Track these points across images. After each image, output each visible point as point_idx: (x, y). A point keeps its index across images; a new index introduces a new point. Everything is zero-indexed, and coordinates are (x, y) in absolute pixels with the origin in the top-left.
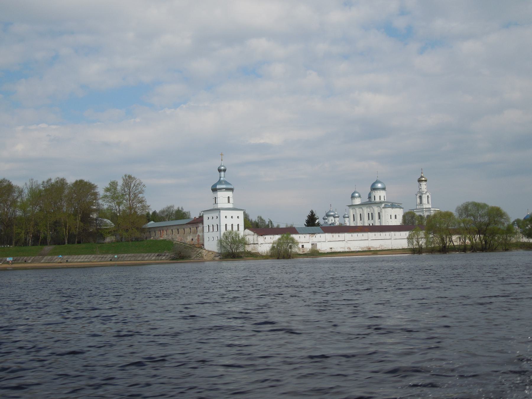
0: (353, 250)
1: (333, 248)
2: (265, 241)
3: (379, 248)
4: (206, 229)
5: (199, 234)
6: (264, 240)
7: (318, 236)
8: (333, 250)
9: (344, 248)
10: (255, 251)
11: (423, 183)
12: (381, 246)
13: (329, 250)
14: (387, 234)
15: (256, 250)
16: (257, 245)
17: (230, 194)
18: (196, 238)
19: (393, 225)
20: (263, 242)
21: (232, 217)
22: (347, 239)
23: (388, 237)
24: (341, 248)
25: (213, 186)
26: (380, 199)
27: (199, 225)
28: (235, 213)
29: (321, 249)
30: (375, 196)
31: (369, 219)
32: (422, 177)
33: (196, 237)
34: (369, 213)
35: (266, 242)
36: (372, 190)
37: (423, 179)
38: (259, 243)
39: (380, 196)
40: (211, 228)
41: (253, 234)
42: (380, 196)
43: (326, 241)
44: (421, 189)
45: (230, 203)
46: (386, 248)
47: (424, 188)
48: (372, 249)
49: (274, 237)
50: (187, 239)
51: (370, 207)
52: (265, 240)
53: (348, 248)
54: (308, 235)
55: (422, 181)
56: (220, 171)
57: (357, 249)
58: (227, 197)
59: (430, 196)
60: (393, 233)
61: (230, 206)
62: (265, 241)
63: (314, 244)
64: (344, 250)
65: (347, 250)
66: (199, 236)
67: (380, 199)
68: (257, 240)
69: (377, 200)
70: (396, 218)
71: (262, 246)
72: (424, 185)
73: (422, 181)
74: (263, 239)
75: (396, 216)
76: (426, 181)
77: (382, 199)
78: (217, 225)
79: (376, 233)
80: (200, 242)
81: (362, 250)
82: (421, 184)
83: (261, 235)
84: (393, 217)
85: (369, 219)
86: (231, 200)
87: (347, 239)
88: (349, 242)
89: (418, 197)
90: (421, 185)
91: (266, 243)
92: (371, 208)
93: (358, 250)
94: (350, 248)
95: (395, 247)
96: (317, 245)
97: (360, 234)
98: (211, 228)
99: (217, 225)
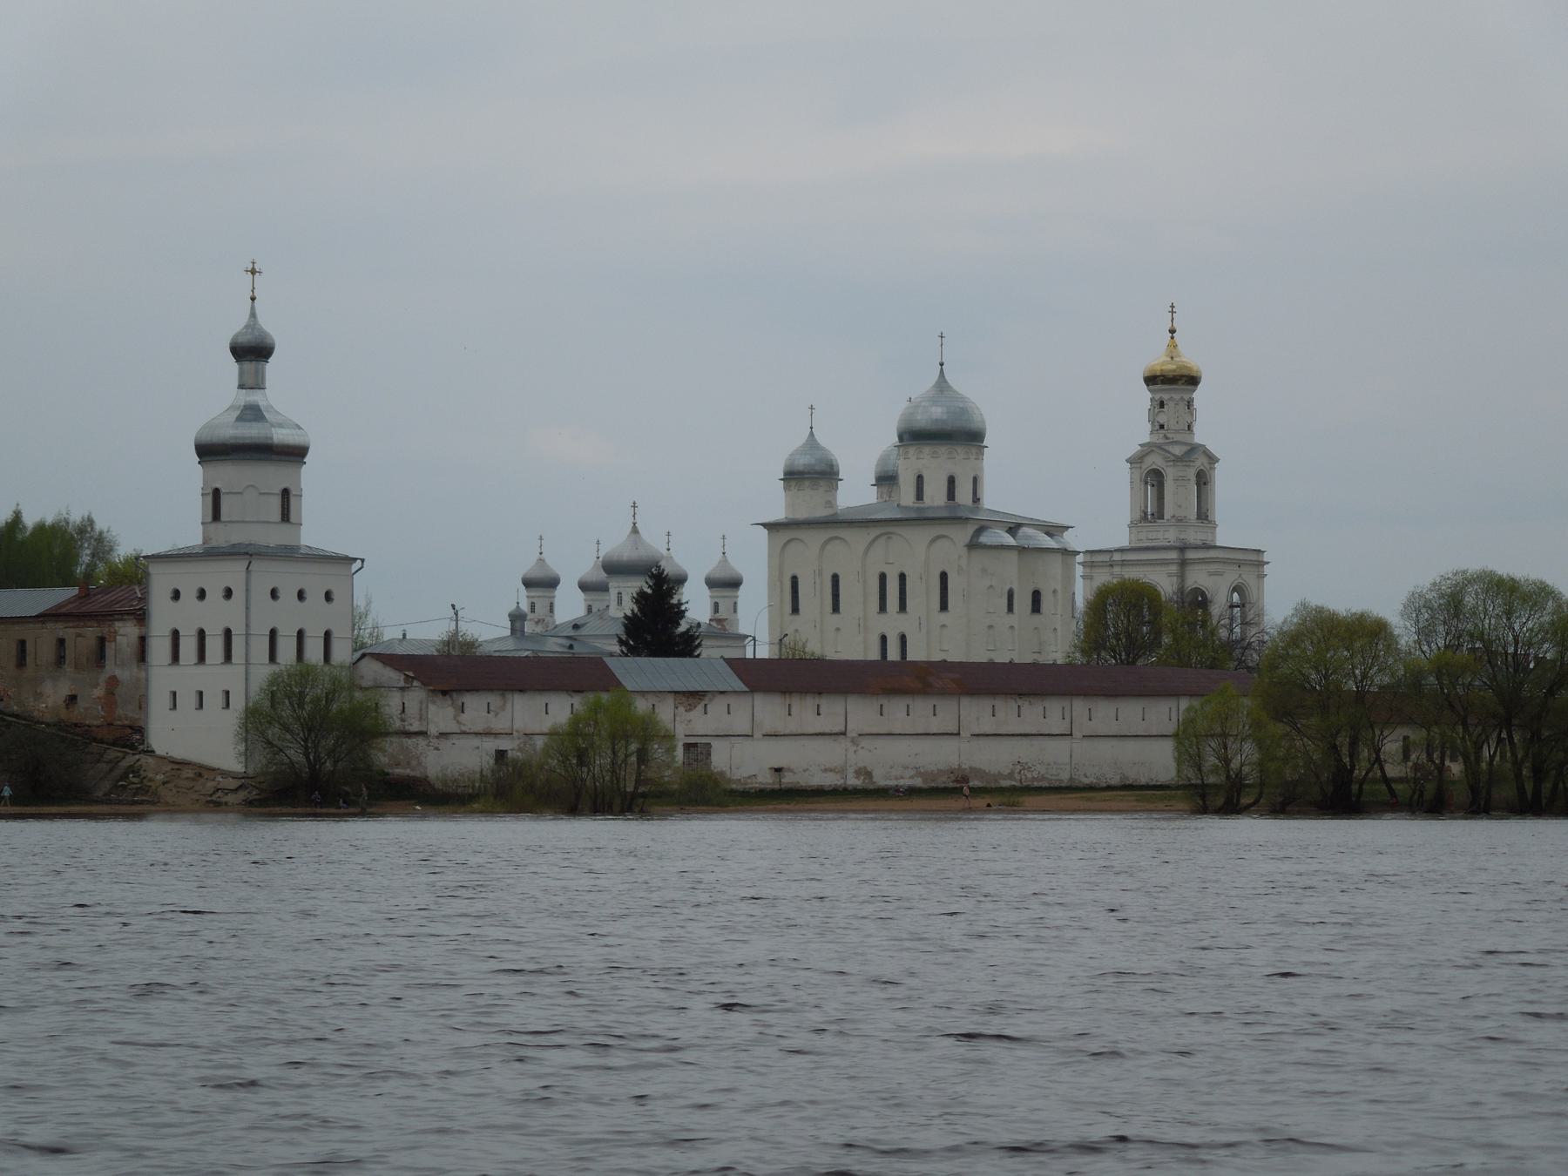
0: (881, 781)
1: (790, 770)
3: (1011, 776)
4: (159, 649)
5: (118, 672)
6: (455, 718)
7: (717, 706)
8: (788, 780)
9: (842, 771)
10: (408, 771)
13: (766, 780)
14: (1055, 707)
15: (414, 763)
16: (421, 741)
18: (99, 692)
20: (452, 727)
21: (301, 595)
22: (854, 727)
23: (1058, 726)
24: (826, 770)
26: (951, 494)
27: (117, 624)
29: (728, 773)
30: (920, 479)
31: (883, 608)
33: (96, 685)
34: (883, 578)
35: (463, 728)
38: (433, 730)
39: (951, 481)
40: (188, 647)
41: (402, 684)
42: (951, 481)
43: (758, 735)
45: (291, 520)
46: (1043, 778)
48: (975, 783)
49: (503, 708)
50: (38, 696)
52: (463, 717)
53: (858, 773)
54: (670, 700)
57: (902, 778)
58: (278, 490)
60: (1079, 706)
62: (458, 722)
63: (695, 745)
64: (840, 782)
65: (853, 781)
66: (113, 682)
67: (951, 494)
68: (422, 717)
70: (1036, 606)
71: (445, 744)
74: (450, 711)
75: (1036, 597)
78: (228, 633)
79: (999, 703)
80: (120, 711)
81: (925, 786)
83: (445, 693)
84: (1023, 602)
85: (883, 608)
87: (854, 727)
88: (865, 742)
91: (464, 733)
93: (905, 782)
94: (869, 774)
95: (1085, 776)
96: (710, 754)
97: (921, 706)
98: (188, 647)
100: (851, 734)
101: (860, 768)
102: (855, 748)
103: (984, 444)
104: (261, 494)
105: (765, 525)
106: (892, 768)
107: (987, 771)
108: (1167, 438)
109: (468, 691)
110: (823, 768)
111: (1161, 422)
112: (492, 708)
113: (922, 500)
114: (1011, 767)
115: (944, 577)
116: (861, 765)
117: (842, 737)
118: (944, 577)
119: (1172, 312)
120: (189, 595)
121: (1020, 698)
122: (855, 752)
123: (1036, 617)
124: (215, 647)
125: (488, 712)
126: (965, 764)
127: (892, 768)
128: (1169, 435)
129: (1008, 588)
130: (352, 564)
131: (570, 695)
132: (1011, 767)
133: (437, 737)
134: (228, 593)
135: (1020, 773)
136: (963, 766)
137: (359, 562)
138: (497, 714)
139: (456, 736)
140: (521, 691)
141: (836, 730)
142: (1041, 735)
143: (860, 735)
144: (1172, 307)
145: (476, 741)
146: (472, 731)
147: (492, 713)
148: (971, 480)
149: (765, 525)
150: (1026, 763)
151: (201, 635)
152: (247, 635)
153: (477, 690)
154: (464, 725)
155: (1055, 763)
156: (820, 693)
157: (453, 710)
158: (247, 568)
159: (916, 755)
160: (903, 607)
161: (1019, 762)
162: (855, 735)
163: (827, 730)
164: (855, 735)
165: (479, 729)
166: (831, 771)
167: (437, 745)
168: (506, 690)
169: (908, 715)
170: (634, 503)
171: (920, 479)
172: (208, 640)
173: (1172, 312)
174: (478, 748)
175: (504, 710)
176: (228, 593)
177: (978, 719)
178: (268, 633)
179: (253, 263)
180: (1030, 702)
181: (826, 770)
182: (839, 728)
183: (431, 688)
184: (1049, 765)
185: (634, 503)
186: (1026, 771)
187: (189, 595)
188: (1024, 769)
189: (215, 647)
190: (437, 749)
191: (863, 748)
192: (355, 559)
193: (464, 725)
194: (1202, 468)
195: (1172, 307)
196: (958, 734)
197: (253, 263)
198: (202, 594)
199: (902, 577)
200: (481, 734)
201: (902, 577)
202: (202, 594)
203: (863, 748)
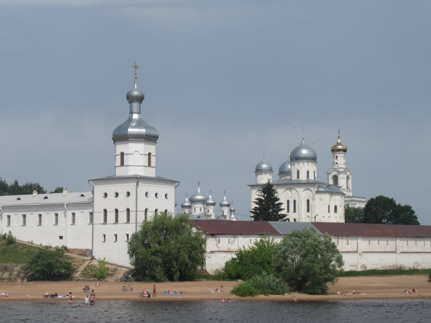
2: (218, 247)
6: (216, 245)
9: (356, 266)
11: (341, 155)
12: (416, 265)
17: (151, 148)
19: (332, 222)
20: (215, 249)
22: (361, 249)
24: (351, 266)
25: (119, 129)
26: (308, 176)
28: (162, 189)
30: (298, 172)
32: (338, 144)
36: (294, 159)
37: (340, 147)
39: (308, 172)
40: (111, 217)
42: (308, 172)
44: (337, 163)
47: (342, 163)
49: (234, 241)
51: (291, 189)
52: (219, 245)
55: (339, 150)
56: (130, 99)
58: (147, 153)
59: (350, 177)
61: (151, 173)
62: (218, 247)
65: (360, 269)
67: (308, 176)
69: (303, 177)
70: (336, 211)
72: (341, 160)
73: (339, 150)
75: (336, 207)
76: (345, 151)
77: (311, 177)
78: (128, 210)
82: (338, 155)
84: (332, 209)
86: (153, 159)
87: (361, 249)
88: (364, 255)
89: (330, 177)
90: (337, 157)
92: (293, 191)
94: (365, 267)
98: (111, 217)
99: (128, 210)
100: (359, 252)
101: (363, 265)
102: (360, 257)
103: (317, 161)
104: (140, 154)
105: (250, 186)
106: (373, 265)
107: (406, 266)
108: (338, 167)
109: (221, 234)
110: (350, 265)
111: (336, 162)
112: (230, 241)
113: (299, 178)
114: (414, 264)
115: (308, 201)
116: (363, 264)
117: (356, 253)
118: (308, 201)
119: (339, 132)
120: (111, 195)
121: (416, 238)
122: (361, 259)
123: (336, 214)
124: (123, 216)
125: (229, 243)
126: (398, 263)
127: (373, 265)
128: (339, 166)
129: (328, 205)
130: (175, 183)
131: (259, 236)
132: (414, 264)
133: (210, 253)
134: (128, 194)
135: (416, 267)
136: (398, 264)
137: (177, 183)
138: (232, 244)
139: (217, 252)
140: (241, 234)
141: (354, 250)
142: (387, 252)
143: (362, 252)
144: (339, 130)
145: (224, 255)
146: (223, 250)
147: (230, 243)
148: (313, 172)
149: (250, 186)
150: (419, 263)
151: (117, 211)
152: (136, 211)
153: (224, 234)
154: (220, 248)
155: (428, 263)
156: (348, 236)
157: (216, 242)
158: (137, 184)
159: (382, 260)
160: (295, 211)
161: (416, 263)
162: (361, 252)
163: (351, 250)
164: (361, 252)
165: (225, 249)
166: (352, 266)
167: (209, 256)
168: (236, 234)
169: (379, 244)
170: (199, 182)
171: (298, 172)
172: (119, 214)
173: (339, 132)
174: (225, 257)
175: (235, 242)
176: (128, 194)
177: (402, 246)
178: (145, 211)
179: (136, 64)
180: (419, 240)
181: (351, 266)
182: (355, 249)
183: (208, 233)
184: (426, 263)
185: (199, 182)
186: (419, 266)
187: (111, 195)
188: (418, 265)
189: (123, 216)
190: (210, 258)
191: (363, 257)
192: (176, 182)
193: (220, 248)
194: (348, 175)
195: (339, 130)
196: (396, 252)
197: (136, 64)
198: (117, 194)
199: (295, 201)
200: (226, 252)
201: (295, 201)
202: (117, 194)
203: (363, 257)
